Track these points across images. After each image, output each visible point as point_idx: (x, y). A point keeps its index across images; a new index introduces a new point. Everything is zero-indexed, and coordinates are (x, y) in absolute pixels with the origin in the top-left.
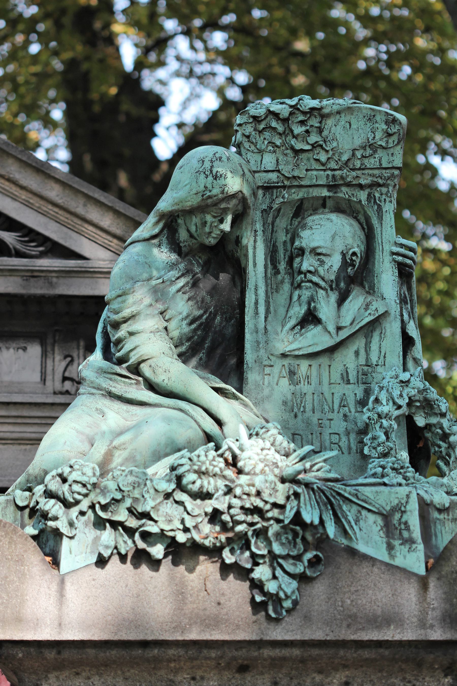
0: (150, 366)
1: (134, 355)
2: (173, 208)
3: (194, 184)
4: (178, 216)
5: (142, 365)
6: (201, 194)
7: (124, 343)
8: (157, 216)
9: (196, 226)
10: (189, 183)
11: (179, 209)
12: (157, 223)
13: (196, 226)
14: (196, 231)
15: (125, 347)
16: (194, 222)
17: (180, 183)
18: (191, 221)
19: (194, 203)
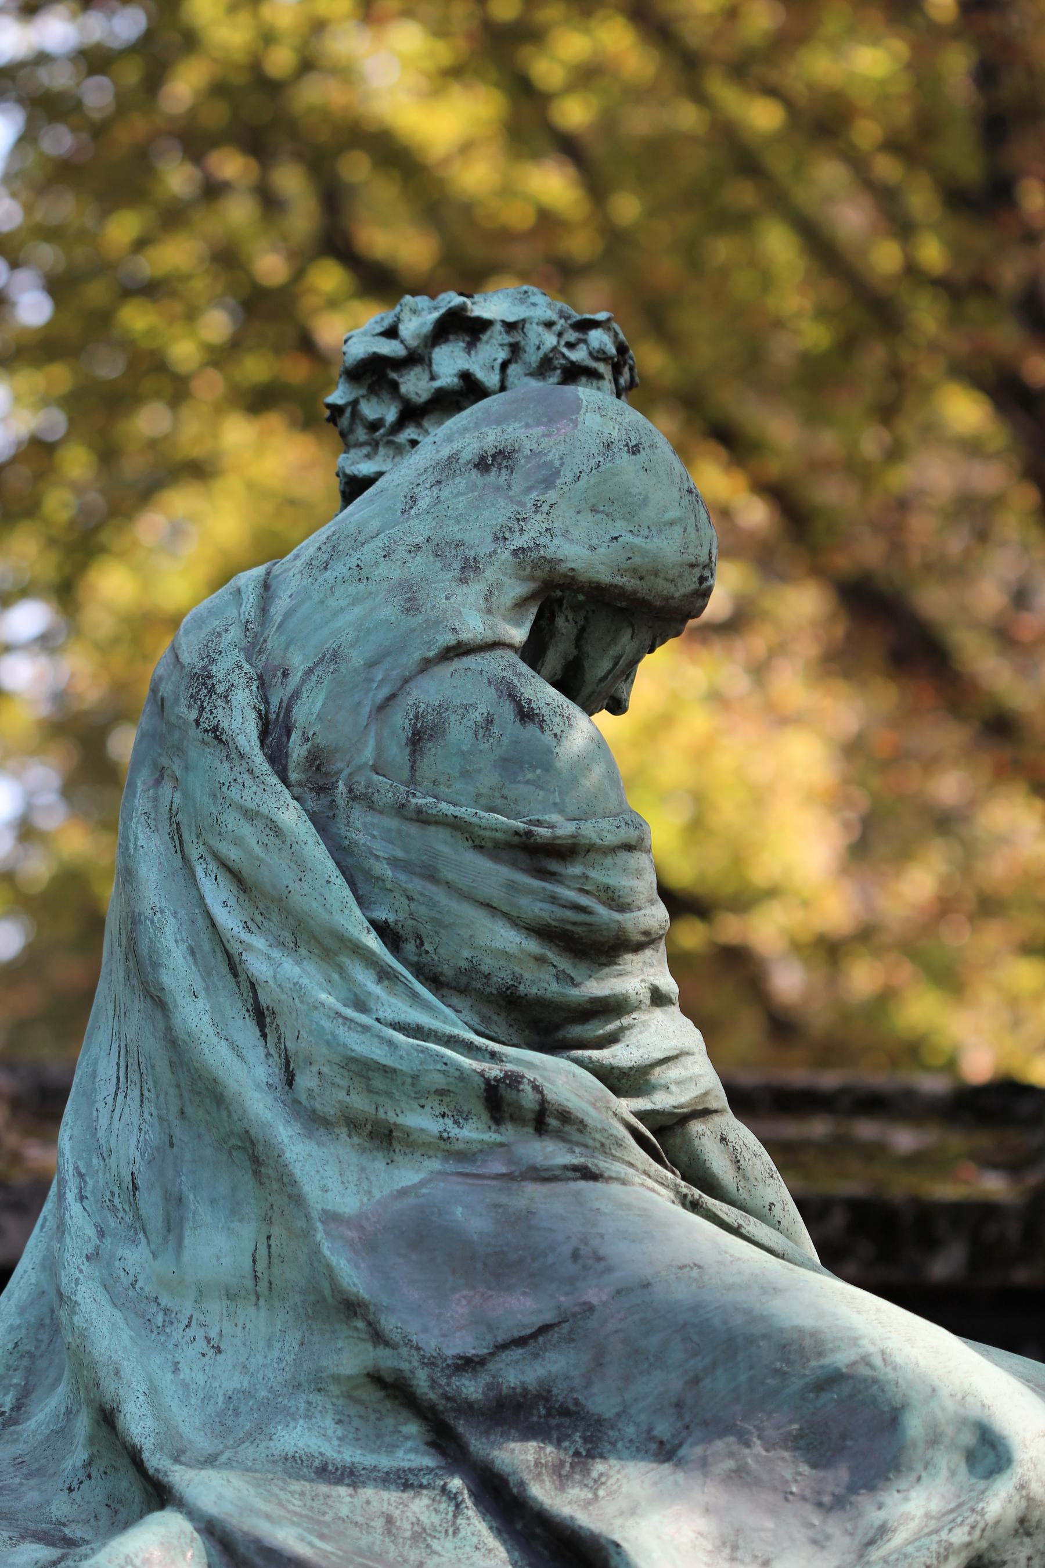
0: (723, 1139)
1: (678, 1083)
2: (618, 580)
3: (691, 529)
4: (560, 601)
5: (696, 1127)
6: (697, 572)
7: (626, 1021)
8: (531, 578)
9: (616, 664)
10: (680, 519)
11: (635, 592)
12: (521, 604)
13: (616, 664)
14: (604, 679)
15: (631, 1038)
16: (614, 651)
17: (645, 502)
18: (614, 641)
19: (677, 595)
